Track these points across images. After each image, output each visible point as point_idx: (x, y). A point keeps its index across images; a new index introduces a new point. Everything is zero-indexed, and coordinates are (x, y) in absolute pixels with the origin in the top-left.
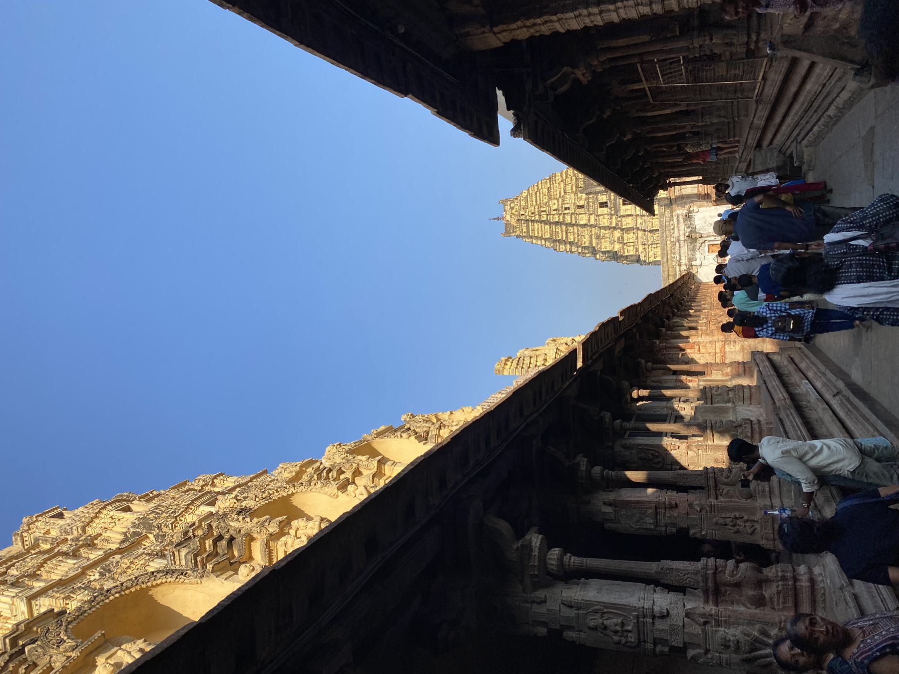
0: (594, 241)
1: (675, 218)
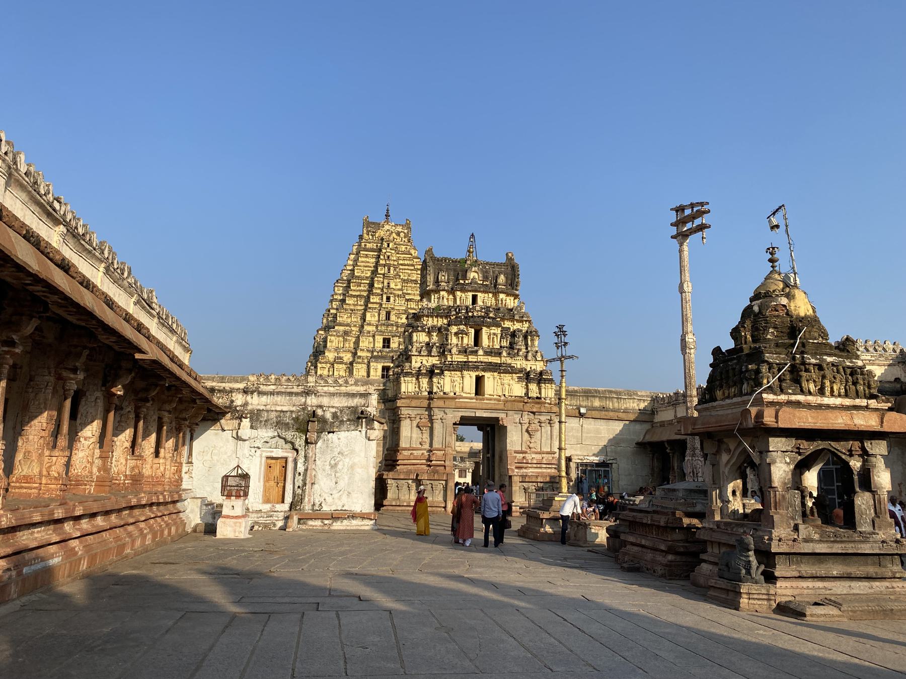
0: (342, 328)
1: (361, 389)
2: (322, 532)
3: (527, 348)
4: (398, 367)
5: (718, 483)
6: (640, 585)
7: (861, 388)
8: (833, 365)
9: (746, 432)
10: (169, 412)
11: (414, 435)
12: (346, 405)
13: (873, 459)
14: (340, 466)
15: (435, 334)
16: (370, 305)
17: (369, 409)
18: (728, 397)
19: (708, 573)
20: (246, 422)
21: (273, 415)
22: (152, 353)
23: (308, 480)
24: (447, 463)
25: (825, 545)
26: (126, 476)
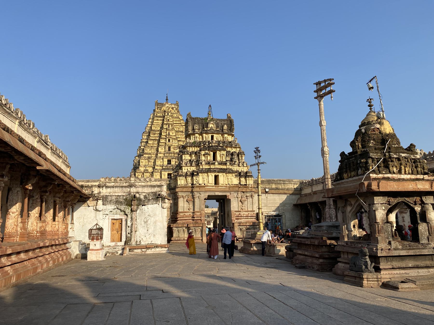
0: (147, 156)
1: (158, 183)
2: (141, 255)
3: (239, 161)
4: (176, 172)
5: (346, 222)
6: (308, 276)
7: (419, 169)
8: (405, 158)
9: (361, 195)
10: (59, 198)
11: (185, 206)
12: (151, 191)
13: (427, 206)
14: (149, 222)
15: (193, 155)
16: (160, 144)
17: (162, 193)
18: (351, 177)
19: (342, 268)
20: (100, 202)
21: (114, 198)
22: (45, 166)
23: (133, 229)
24: (202, 218)
25: (405, 251)
26: (37, 231)
